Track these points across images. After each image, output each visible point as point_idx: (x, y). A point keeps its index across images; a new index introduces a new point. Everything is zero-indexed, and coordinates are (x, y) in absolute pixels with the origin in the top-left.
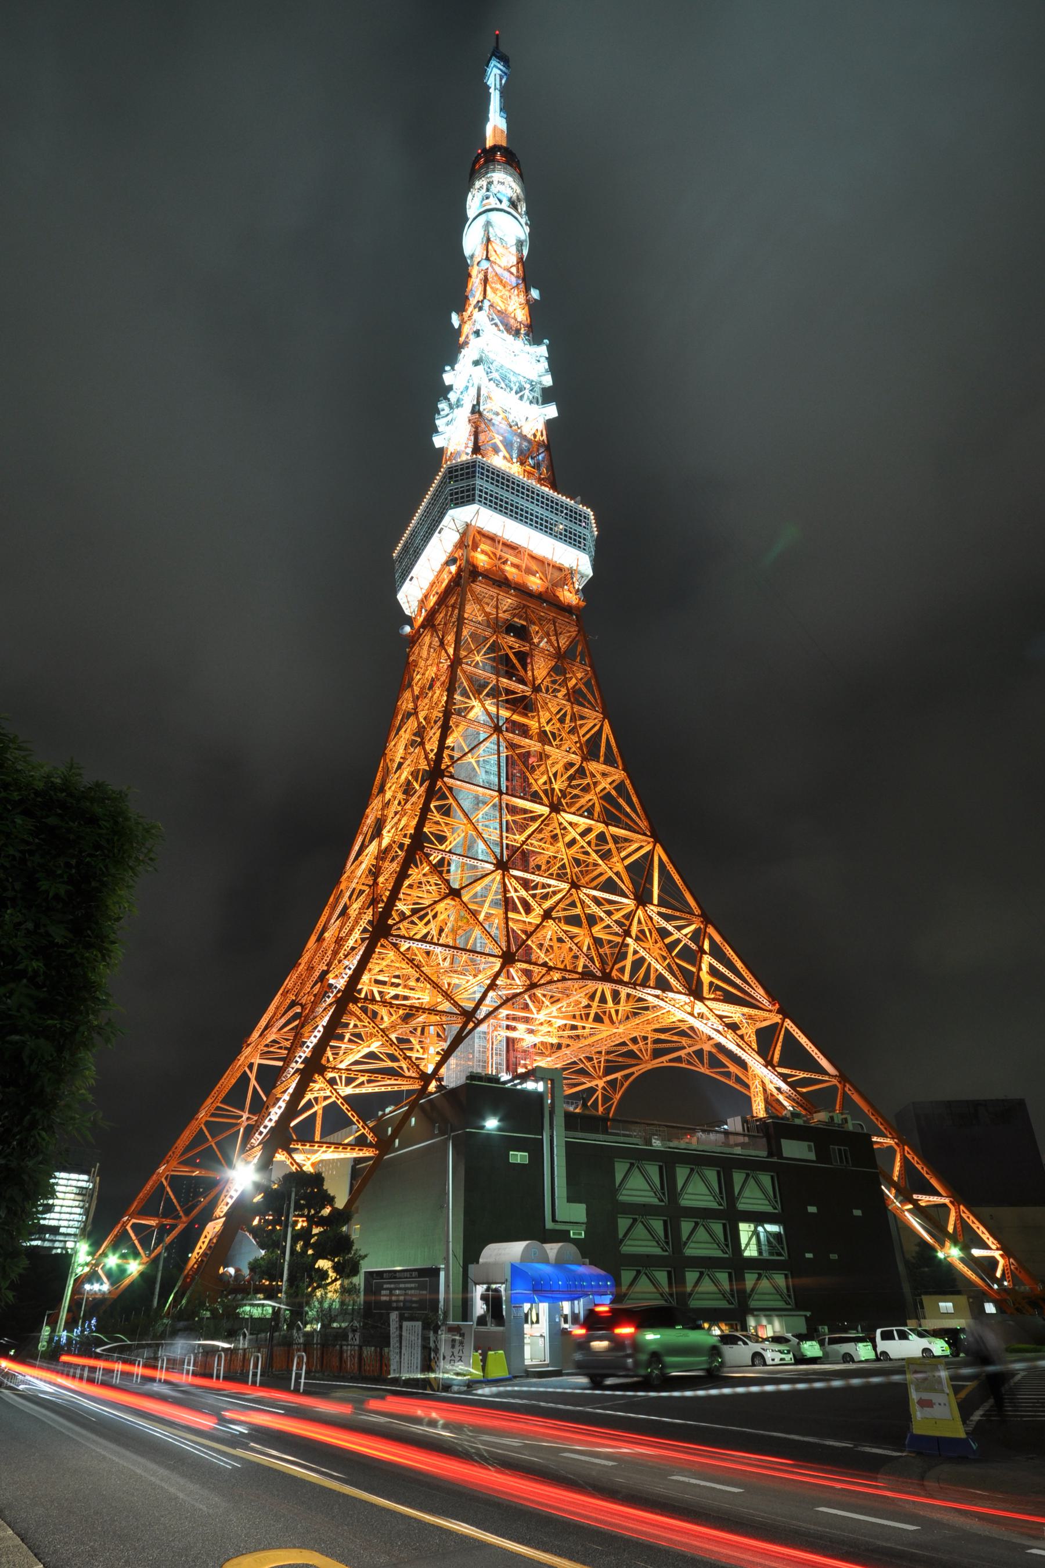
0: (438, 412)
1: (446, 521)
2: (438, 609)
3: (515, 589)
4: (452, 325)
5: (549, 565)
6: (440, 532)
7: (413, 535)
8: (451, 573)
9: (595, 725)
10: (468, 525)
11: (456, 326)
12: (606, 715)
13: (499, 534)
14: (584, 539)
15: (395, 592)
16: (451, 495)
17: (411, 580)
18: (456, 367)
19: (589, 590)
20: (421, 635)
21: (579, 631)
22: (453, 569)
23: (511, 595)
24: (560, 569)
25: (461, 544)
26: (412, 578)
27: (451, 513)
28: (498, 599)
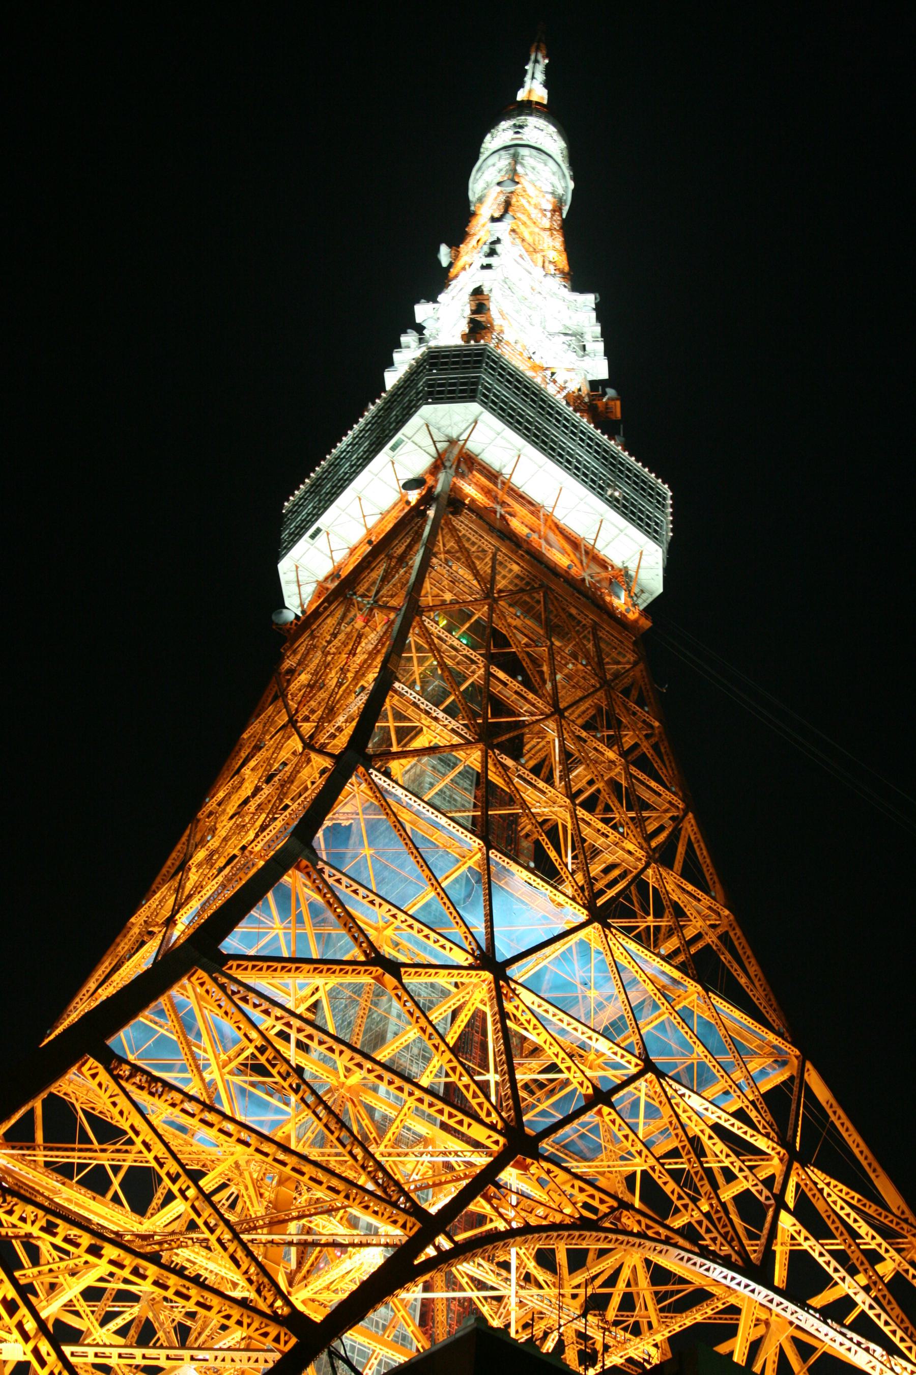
0: (398, 345)
1: (415, 422)
2: (370, 563)
3: (528, 552)
4: (439, 263)
5: (587, 553)
6: (393, 449)
7: (335, 465)
8: (408, 503)
9: (661, 829)
10: (452, 442)
11: (445, 263)
12: (693, 802)
13: (506, 471)
14: (657, 524)
16: (430, 386)
17: (313, 537)
18: (440, 298)
19: (655, 608)
20: (321, 614)
21: (635, 664)
22: (414, 496)
24: (603, 564)
25: (438, 466)
26: (318, 531)
27: (428, 412)
28: (494, 559)
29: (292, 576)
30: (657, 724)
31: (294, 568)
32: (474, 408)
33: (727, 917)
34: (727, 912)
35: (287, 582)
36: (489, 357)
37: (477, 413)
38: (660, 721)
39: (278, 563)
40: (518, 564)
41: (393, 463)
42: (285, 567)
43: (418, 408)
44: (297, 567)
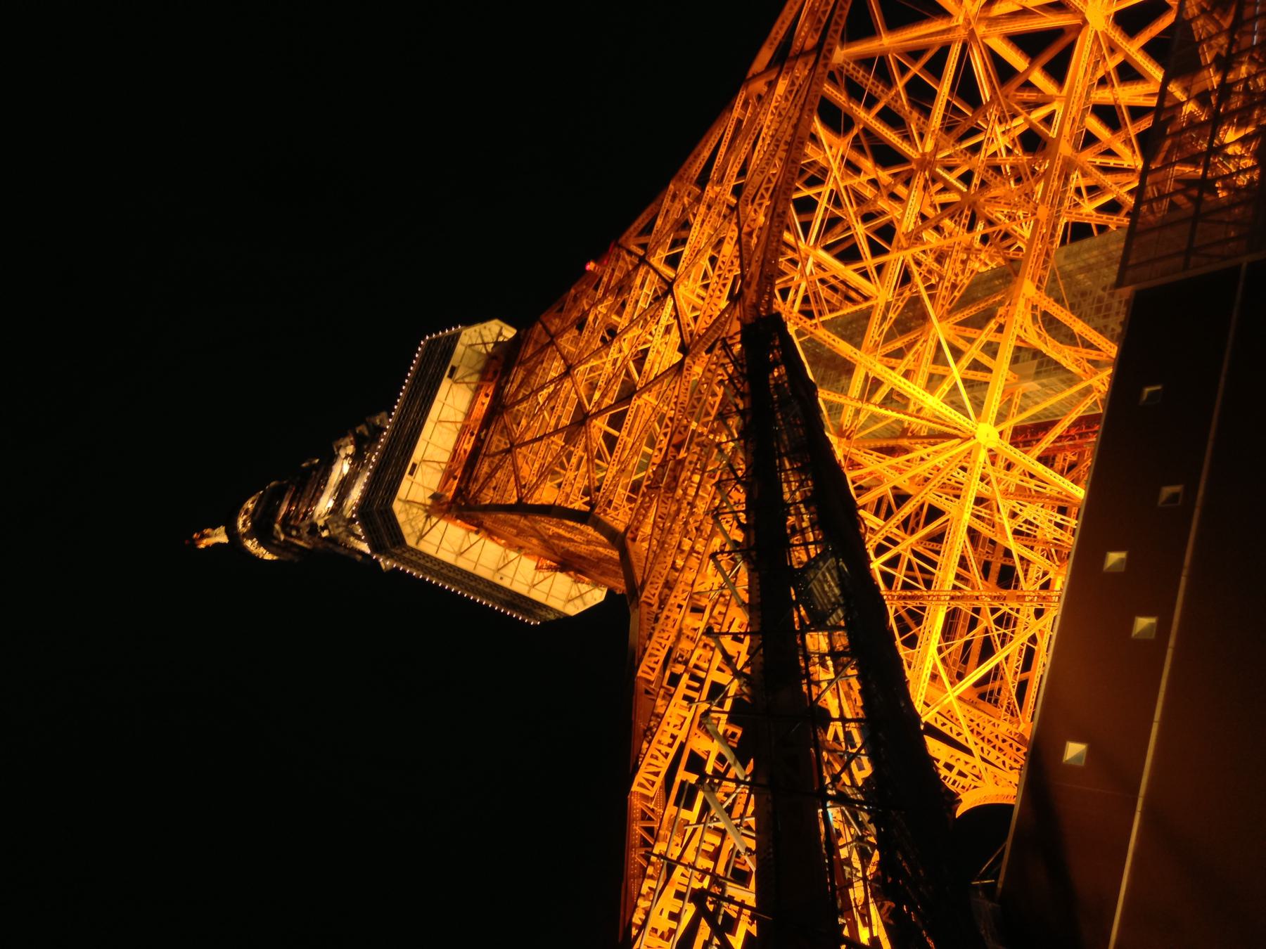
15: (567, 619)
23: (486, 435)
27: (411, 542)
29: (578, 602)
30: (573, 291)
31: (571, 603)
32: (397, 506)
33: (674, 185)
34: (671, 187)
35: (585, 604)
36: (363, 508)
37: (401, 504)
38: (570, 289)
39: (571, 617)
40: (492, 436)
41: (462, 553)
42: (573, 610)
43: (412, 549)
44: (569, 601)
